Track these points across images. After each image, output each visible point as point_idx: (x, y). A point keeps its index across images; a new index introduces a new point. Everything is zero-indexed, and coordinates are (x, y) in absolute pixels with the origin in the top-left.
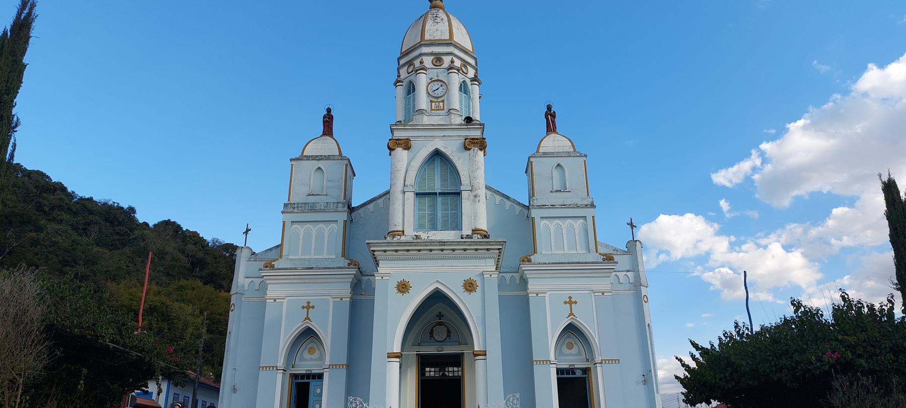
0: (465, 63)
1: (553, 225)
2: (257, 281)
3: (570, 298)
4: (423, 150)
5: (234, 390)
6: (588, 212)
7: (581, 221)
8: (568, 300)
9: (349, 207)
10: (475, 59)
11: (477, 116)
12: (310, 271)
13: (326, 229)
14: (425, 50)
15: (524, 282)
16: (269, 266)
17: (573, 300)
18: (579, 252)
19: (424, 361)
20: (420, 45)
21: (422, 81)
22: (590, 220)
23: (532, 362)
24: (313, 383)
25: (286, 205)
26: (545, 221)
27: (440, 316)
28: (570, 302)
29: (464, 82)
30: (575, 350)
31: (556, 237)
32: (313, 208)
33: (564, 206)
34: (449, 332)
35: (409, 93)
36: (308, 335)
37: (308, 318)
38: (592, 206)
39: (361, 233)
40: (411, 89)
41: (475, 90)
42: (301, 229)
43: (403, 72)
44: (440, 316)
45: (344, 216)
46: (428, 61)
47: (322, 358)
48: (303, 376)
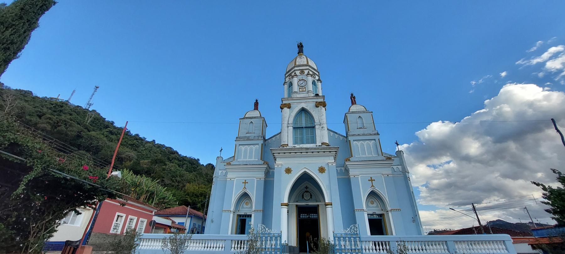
2: (224, 172)
5: (212, 221)
7: (373, 141)
9: (264, 138)
11: (320, 94)
12: (247, 166)
13: (254, 148)
14: (296, 68)
15: (347, 171)
16: (229, 164)
18: (374, 155)
20: (294, 67)
21: (295, 81)
22: (377, 141)
23: (354, 211)
24: (247, 219)
26: (355, 142)
30: (375, 205)
31: (362, 149)
32: (248, 139)
33: (364, 135)
34: (311, 196)
36: (245, 196)
37: (245, 188)
38: (378, 134)
39: (269, 149)
40: (291, 84)
41: (319, 84)
42: (243, 148)
45: (262, 142)
46: (298, 73)
47: (251, 207)
48: (243, 216)
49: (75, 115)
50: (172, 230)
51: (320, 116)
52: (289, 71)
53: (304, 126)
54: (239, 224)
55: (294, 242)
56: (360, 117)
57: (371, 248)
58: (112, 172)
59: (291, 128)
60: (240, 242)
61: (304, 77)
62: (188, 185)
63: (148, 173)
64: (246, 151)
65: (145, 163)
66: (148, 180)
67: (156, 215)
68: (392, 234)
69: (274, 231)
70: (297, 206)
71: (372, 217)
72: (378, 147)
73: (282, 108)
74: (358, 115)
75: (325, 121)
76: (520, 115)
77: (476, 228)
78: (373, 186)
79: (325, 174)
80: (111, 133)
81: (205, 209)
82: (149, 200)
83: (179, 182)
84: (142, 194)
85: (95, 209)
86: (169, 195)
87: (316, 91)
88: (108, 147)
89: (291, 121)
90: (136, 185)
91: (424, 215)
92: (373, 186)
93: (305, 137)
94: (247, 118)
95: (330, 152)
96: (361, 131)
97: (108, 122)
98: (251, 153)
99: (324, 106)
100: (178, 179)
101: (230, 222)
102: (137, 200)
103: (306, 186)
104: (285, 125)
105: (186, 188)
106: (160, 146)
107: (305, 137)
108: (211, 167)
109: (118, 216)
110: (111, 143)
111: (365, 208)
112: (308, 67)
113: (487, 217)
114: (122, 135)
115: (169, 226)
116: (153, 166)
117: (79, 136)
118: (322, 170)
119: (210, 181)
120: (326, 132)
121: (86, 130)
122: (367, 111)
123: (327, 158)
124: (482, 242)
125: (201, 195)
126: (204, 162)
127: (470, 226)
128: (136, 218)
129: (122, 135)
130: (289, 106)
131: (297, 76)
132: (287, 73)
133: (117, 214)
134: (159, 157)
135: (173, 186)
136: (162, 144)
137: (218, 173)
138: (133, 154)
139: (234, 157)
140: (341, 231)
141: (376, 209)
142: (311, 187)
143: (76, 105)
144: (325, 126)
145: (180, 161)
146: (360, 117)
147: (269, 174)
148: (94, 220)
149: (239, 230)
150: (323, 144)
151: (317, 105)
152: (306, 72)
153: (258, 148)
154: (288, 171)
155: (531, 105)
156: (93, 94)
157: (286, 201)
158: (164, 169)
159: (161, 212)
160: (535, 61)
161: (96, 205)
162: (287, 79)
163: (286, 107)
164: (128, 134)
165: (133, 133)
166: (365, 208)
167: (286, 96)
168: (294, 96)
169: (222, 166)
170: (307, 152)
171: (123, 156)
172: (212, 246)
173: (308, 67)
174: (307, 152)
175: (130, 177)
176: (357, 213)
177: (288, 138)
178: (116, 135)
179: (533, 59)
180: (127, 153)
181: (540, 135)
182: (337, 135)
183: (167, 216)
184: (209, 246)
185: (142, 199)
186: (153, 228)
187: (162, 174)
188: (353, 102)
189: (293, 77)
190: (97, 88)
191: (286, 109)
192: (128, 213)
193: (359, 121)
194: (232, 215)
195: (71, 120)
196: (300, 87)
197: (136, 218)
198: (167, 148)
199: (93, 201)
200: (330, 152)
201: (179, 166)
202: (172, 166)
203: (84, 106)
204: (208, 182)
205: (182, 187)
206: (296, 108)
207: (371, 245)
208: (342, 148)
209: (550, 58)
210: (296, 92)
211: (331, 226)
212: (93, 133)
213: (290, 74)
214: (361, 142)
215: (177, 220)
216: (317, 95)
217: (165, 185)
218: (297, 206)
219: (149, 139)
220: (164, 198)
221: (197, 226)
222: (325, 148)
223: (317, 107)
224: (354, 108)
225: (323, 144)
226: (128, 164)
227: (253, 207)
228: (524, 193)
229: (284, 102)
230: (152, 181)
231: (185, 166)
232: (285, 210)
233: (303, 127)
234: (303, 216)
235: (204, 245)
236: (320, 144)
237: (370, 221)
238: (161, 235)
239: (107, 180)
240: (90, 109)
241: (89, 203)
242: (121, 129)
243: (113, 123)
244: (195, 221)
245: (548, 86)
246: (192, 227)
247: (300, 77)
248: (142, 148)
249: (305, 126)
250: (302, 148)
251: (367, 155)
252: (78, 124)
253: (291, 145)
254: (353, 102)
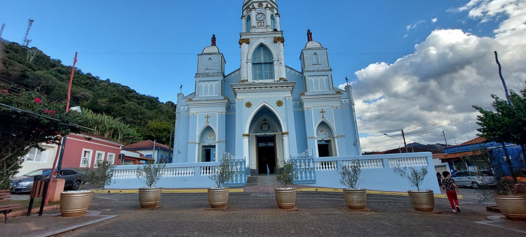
0: (273, 7)
1: (313, 79)
2: (186, 107)
5: (179, 152)
6: (329, 73)
7: (326, 77)
9: (224, 74)
10: (277, 6)
11: (279, 30)
12: (208, 102)
13: (214, 84)
15: (301, 104)
16: (190, 100)
18: (326, 90)
19: (259, 139)
21: (253, 14)
23: (306, 138)
25: (196, 74)
27: (265, 120)
28: (322, 112)
29: (272, 15)
30: (324, 133)
31: (315, 84)
32: (208, 75)
33: (318, 71)
34: (269, 127)
35: (248, 21)
36: (208, 129)
37: (207, 122)
38: (331, 70)
39: (229, 85)
40: (249, 18)
41: (277, 19)
42: (203, 84)
43: (245, 13)
44: (265, 120)
45: (221, 78)
46: (256, 5)
47: (215, 139)
48: (208, 146)
49: (12, 53)
50: (141, 161)
51: (278, 51)
52: (246, 4)
53: (263, 62)
54: (205, 153)
55: (254, 166)
56: (315, 53)
57: (318, 167)
58: (70, 108)
59: (250, 64)
60: (208, 168)
61: (262, 10)
62: (150, 121)
63: (108, 111)
64: (206, 87)
65: (103, 102)
66: (108, 118)
67: (123, 149)
68: (336, 155)
69: (237, 158)
70: (256, 136)
71: (321, 143)
72: (331, 83)
73: (241, 44)
74: (313, 52)
75: (283, 56)
76: (442, 56)
77: (401, 149)
78: (323, 117)
79: (283, 107)
80: (60, 71)
81: (170, 143)
82: (113, 137)
83: (141, 119)
84: (105, 131)
85: (59, 144)
86: (133, 131)
87: (274, 26)
88: (60, 87)
89: (250, 57)
90: (97, 123)
91: (362, 141)
92: (323, 117)
93: (264, 73)
94: (205, 54)
95: (287, 87)
96: (316, 68)
97: (54, 60)
98: (212, 89)
99: (283, 42)
100: (140, 116)
101: (196, 152)
102: (102, 136)
103: (265, 118)
104: (244, 60)
105: (149, 125)
106: (115, 85)
107: (264, 73)
108: (172, 106)
109: (85, 152)
110: (62, 83)
111: (315, 136)
113: (409, 140)
114: (73, 73)
115: (137, 158)
116: (112, 105)
117: (24, 76)
118: (279, 103)
119: (173, 117)
120: (283, 68)
121: (30, 69)
122: (321, 48)
123: (285, 93)
124: (404, 159)
125: (165, 130)
126: (163, 100)
127: (397, 147)
128: (103, 153)
129: (73, 73)
130: (248, 42)
131: (255, 8)
133: (84, 150)
134: (116, 96)
135: (135, 123)
136: (118, 83)
137: (180, 110)
138: (88, 93)
139: (194, 93)
140: (296, 155)
141: (324, 136)
142: (269, 119)
143: (11, 41)
144: (283, 62)
145: (139, 99)
146: (315, 53)
147: (230, 108)
148: (61, 156)
149: (204, 159)
150: (281, 79)
151: (276, 40)
152: (265, 4)
153: (219, 83)
154: (249, 105)
155: (452, 48)
156: (29, 29)
157: (247, 132)
158: (124, 108)
159: (128, 147)
160: (462, 9)
161: (60, 140)
162: (245, 13)
163: (244, 42)
164: (78, 73)
165: (85, 71)
166: (315, 136)
167: (244, 31)
168: (253, 30)
169: (184, 102)
170: (266, 87)
171: (78, 95)
172: (180, 172)
174: (266, 87)
175: (90, 115)
176: (309, 141)
177: (248, 73)
178: (66, 74)
179: (461, 7)
180: (82, 93)
181: (456, 75)
182: (293, 72)
183: (134, 150)
184: (177, 172)
185: (106, 135)
186: (122, 161)
187: (122, 112)
188: (310, 39)
189: (251, 10)
190: (32, 21)
191: (244, 45)
192: (95, 148)
193: (314, 57)
194: (197, 146)
195: (10, 58)
196: (259, 21)
197: (103, 153)
198: (123, 87)
199: (55, 137)
200: (287, 87)
201: (139, 104)
202: (131, 104)
203: (21, 43)
204: (170, 118)
205: (146, 124)
206: (255, 44)
207: (318, 165)
208: (298, 83)
209: (473, 7)
210: (254, 27)
211: (287, 151)
212: (39, 73)
213: (247, 7)
214: (315, 77)
215: (145, 153)
216: (275, 30)
217: (127, 123)
218: (256, 136)
219: (103, 78)
220: (128, 135)
221: (164, 157)
222: (283, 83)
223: (275, 42)
224: (310, 45)
225: (281, 79)
226: (85, 103)
227: (217, 139)
228: (437, 121)
229: (243, 37)
230: (114, 118)
231: (145, 104)
232: (246, 140)
233: (261, 63)
234: (262, 145)
235: (172, 172)
236: (278, 80)
237: (319, 145)
238: (131, 166)
239: (67, 115)
240: (30, 46)
241: (51, 139)
242: (69, 67)
243: (59, 62)
244: (162, 153)
245: (469, 32)
246: (159, 158)
247: (258, 10)
248: (96, 87)
249: (264, 60)
250: (261, 83)
251: (320, 90)
252: (19, 62)
253: (250, 80)
254: (310, 39)
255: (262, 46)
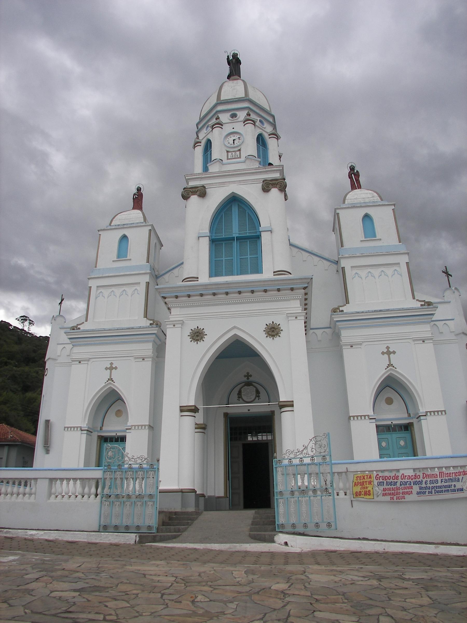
3: (388, 348)
4: (217, 196)
8: (385, 350)
14: (219, 108)
17: (391, 350)
28: (389, 353)
34: (258, 392)
61: (239, 127)
112: (246, 105)
132: (201, 120)
151: (267, 187)
173: (246, 105)
255: (234, 201)
